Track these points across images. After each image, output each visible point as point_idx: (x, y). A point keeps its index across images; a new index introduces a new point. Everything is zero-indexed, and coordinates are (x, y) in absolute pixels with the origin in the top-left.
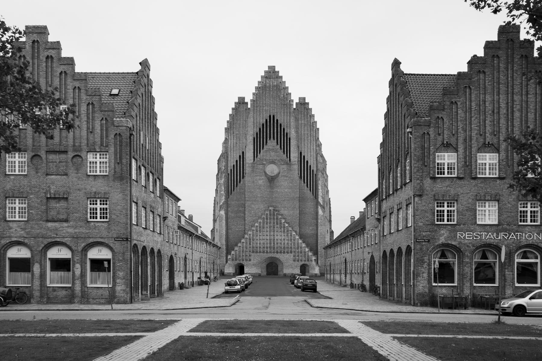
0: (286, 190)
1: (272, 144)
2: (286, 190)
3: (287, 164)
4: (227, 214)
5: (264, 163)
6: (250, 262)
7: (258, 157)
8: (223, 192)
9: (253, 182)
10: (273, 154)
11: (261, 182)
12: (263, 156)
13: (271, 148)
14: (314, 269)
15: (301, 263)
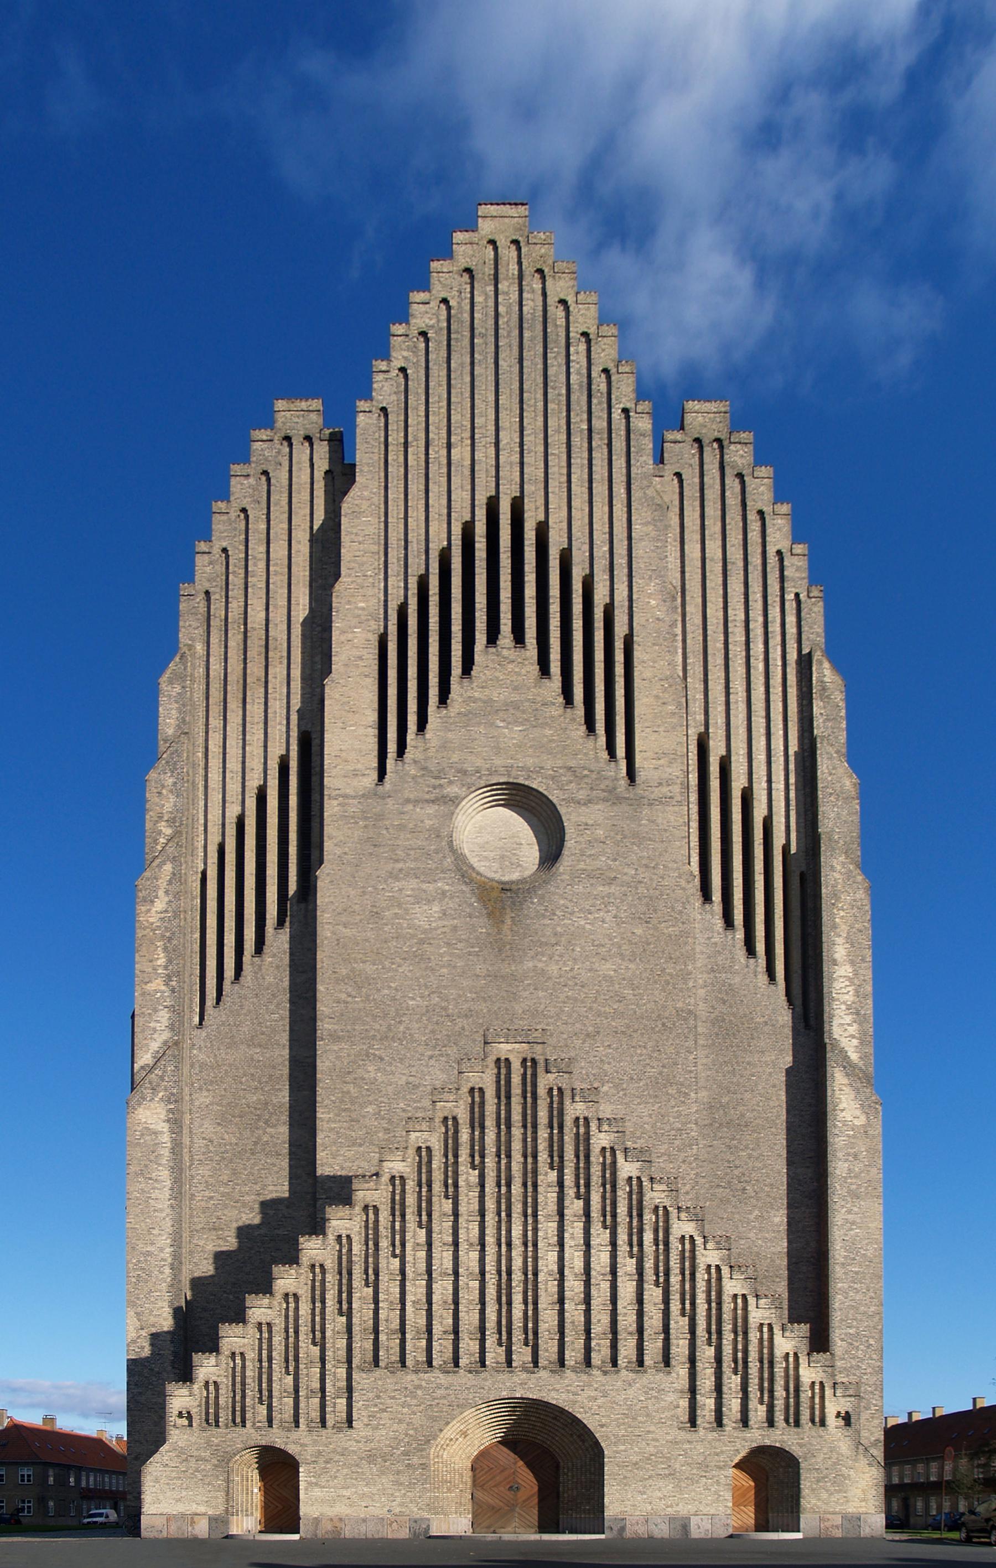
0: (607, 968)
1: (505, 673)
2: (607, 968)
3: (612, 797)
4: (175, 1123)
5: (453, 790)
6: (346, 1440)
7: (410, 753)
8: (157, 985)
9: (376, 915)
10: (512, 734)
11: (426, 916)
12: (444, 746)
13: (499, 695)
14: (840, 1482)
15: (740, 1443)
